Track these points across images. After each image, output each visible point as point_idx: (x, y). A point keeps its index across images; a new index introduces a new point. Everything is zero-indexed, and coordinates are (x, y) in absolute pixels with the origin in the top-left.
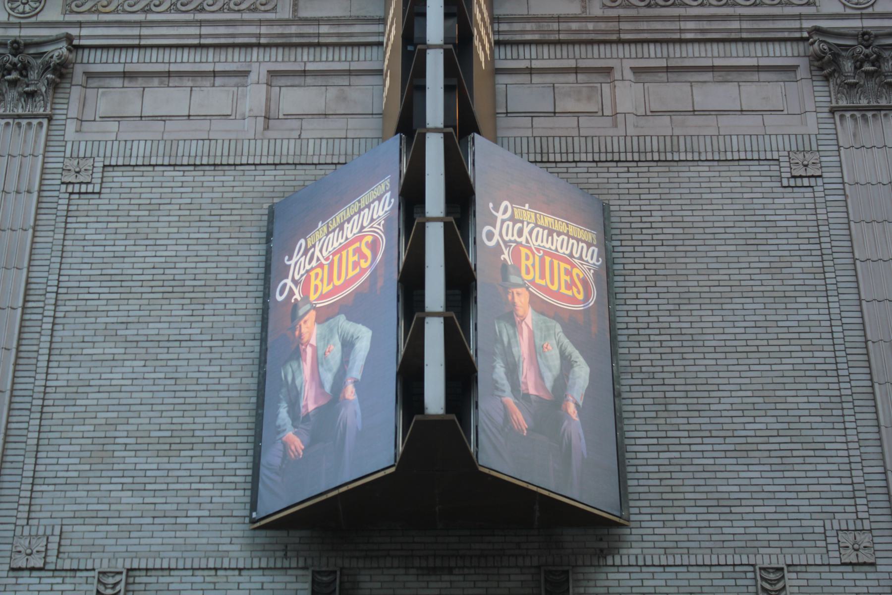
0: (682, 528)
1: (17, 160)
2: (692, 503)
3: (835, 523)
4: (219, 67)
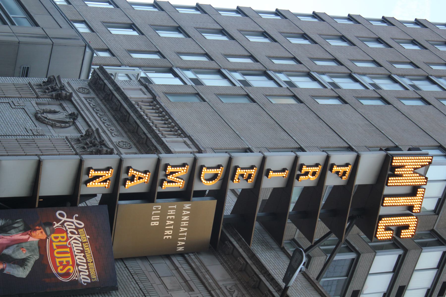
1: (54, 149)
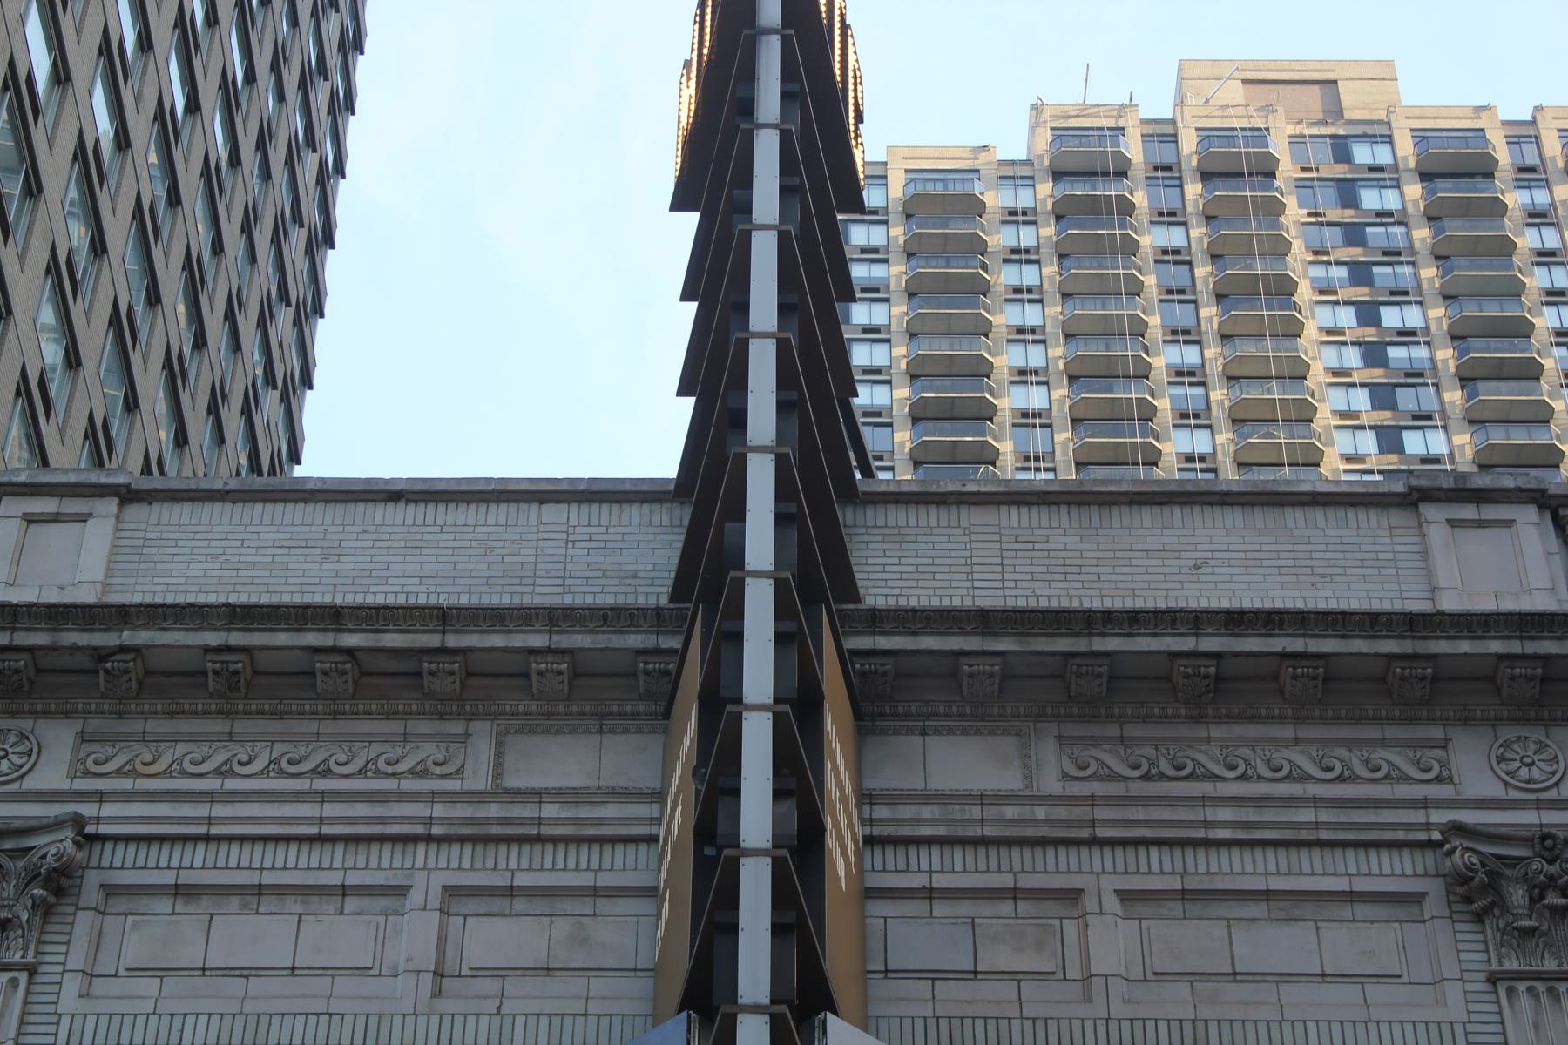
4: (353, 879)
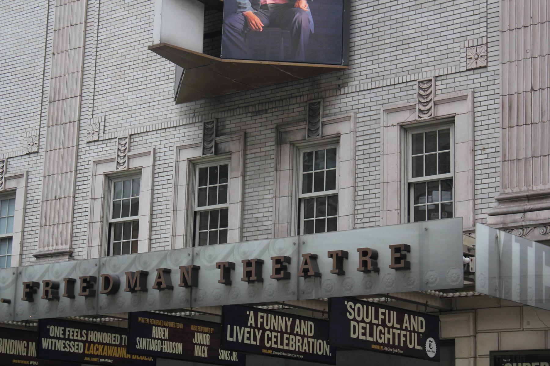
0: (381, 63)
2: (388, 46)
3: (466, 42)
